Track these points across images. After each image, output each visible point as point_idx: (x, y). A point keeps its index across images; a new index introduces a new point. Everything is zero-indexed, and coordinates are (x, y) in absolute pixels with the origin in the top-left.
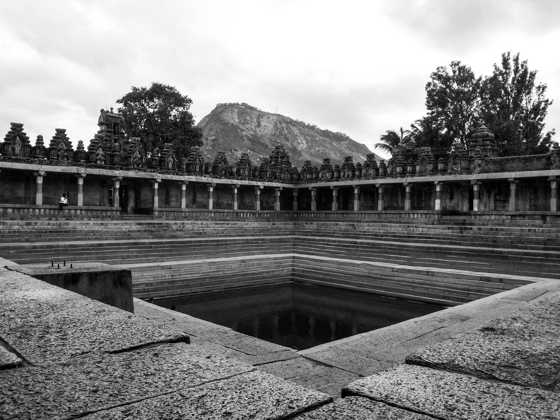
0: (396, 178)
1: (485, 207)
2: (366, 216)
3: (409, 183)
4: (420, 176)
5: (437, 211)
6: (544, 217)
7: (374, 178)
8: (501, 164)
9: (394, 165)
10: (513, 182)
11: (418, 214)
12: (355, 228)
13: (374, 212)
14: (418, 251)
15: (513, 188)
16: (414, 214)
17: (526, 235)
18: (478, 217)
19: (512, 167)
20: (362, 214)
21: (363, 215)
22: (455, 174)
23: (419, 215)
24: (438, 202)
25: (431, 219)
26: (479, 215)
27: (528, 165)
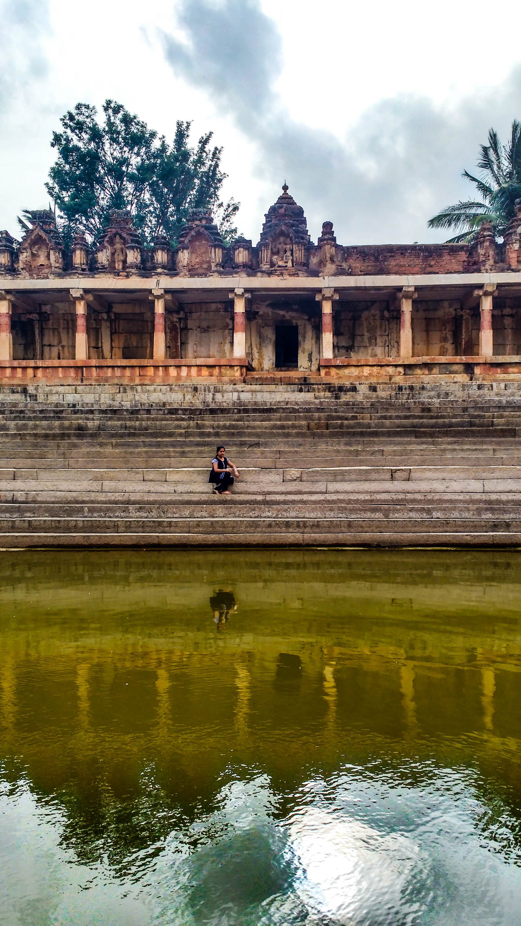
0: (127, 277)
1: (310, 360)
2: (40, 373)
3: (167, 291)
4: (192, 276)
5: (240, 360)
6: (469, 368)
7: (60, 276)
8: (377, 259)
9: (118, 246)
10: (407, 296)
11: (189, 366)
12: (34, 397)
13: (64, 363)
14: (288, 435)
15: (407, 307)
16: (179, 367)
17: (479, 396)
18: (333, 371)
19: (402, 266)
20: (24, 368)
21: (30, 372)
22: (282, 274)
23: (194, 370)
24: (240, 337)
25: (226, 379)
26: (338, 367)
27: (432, 263)
